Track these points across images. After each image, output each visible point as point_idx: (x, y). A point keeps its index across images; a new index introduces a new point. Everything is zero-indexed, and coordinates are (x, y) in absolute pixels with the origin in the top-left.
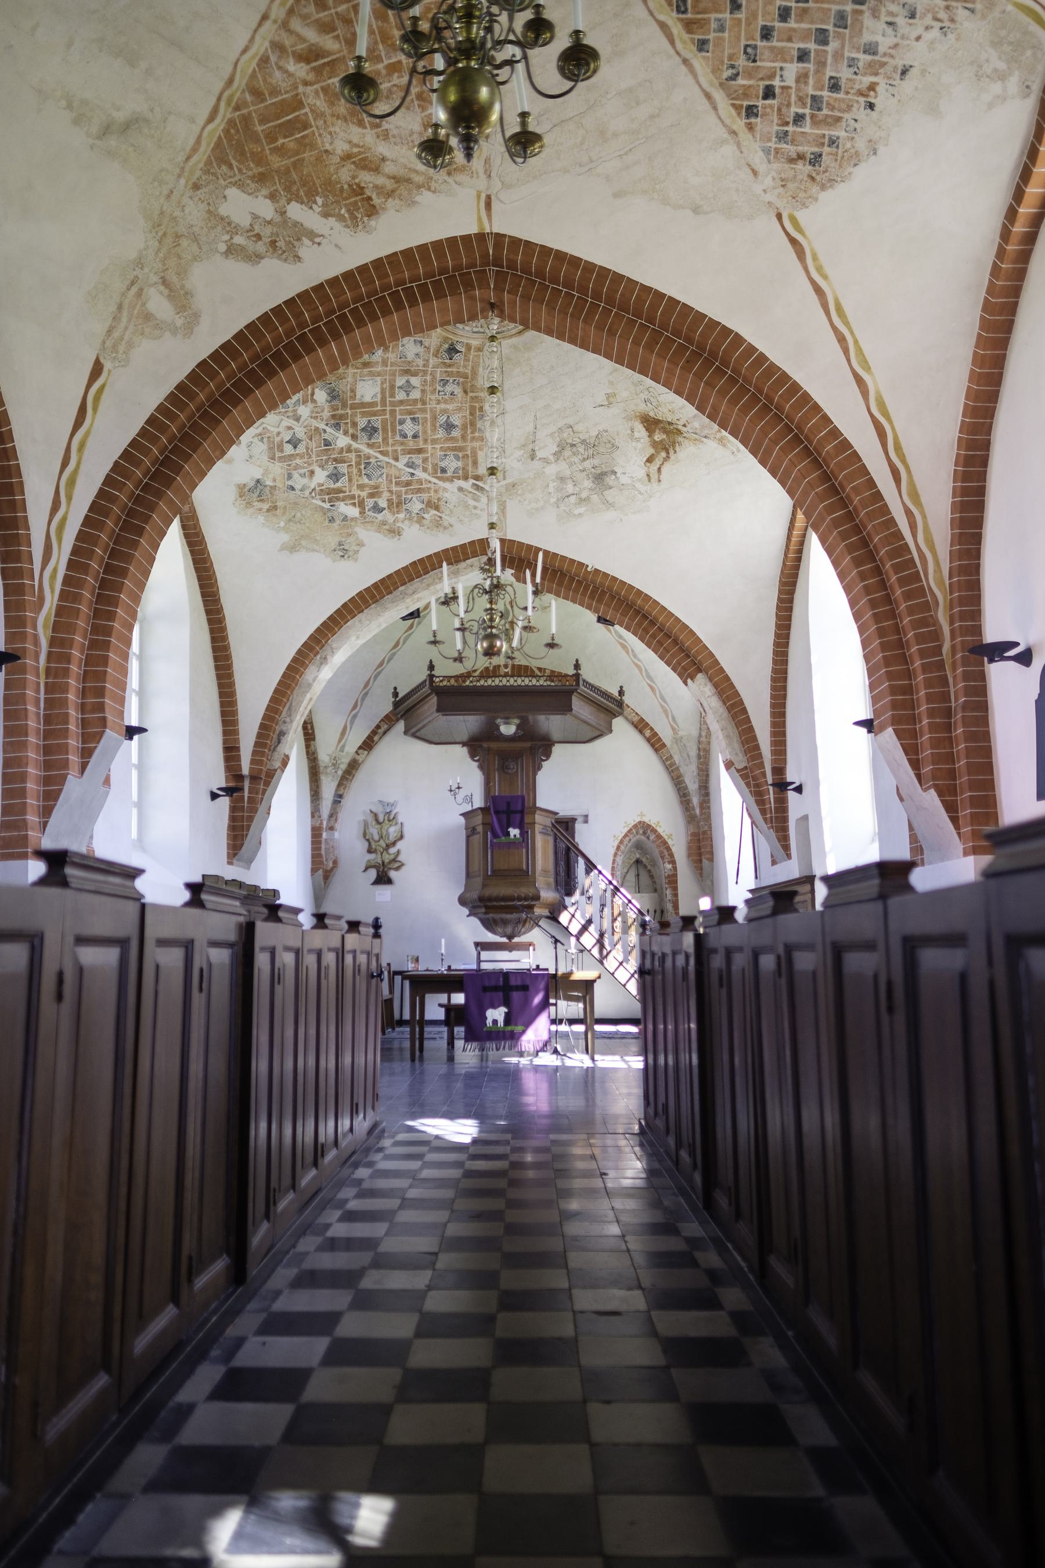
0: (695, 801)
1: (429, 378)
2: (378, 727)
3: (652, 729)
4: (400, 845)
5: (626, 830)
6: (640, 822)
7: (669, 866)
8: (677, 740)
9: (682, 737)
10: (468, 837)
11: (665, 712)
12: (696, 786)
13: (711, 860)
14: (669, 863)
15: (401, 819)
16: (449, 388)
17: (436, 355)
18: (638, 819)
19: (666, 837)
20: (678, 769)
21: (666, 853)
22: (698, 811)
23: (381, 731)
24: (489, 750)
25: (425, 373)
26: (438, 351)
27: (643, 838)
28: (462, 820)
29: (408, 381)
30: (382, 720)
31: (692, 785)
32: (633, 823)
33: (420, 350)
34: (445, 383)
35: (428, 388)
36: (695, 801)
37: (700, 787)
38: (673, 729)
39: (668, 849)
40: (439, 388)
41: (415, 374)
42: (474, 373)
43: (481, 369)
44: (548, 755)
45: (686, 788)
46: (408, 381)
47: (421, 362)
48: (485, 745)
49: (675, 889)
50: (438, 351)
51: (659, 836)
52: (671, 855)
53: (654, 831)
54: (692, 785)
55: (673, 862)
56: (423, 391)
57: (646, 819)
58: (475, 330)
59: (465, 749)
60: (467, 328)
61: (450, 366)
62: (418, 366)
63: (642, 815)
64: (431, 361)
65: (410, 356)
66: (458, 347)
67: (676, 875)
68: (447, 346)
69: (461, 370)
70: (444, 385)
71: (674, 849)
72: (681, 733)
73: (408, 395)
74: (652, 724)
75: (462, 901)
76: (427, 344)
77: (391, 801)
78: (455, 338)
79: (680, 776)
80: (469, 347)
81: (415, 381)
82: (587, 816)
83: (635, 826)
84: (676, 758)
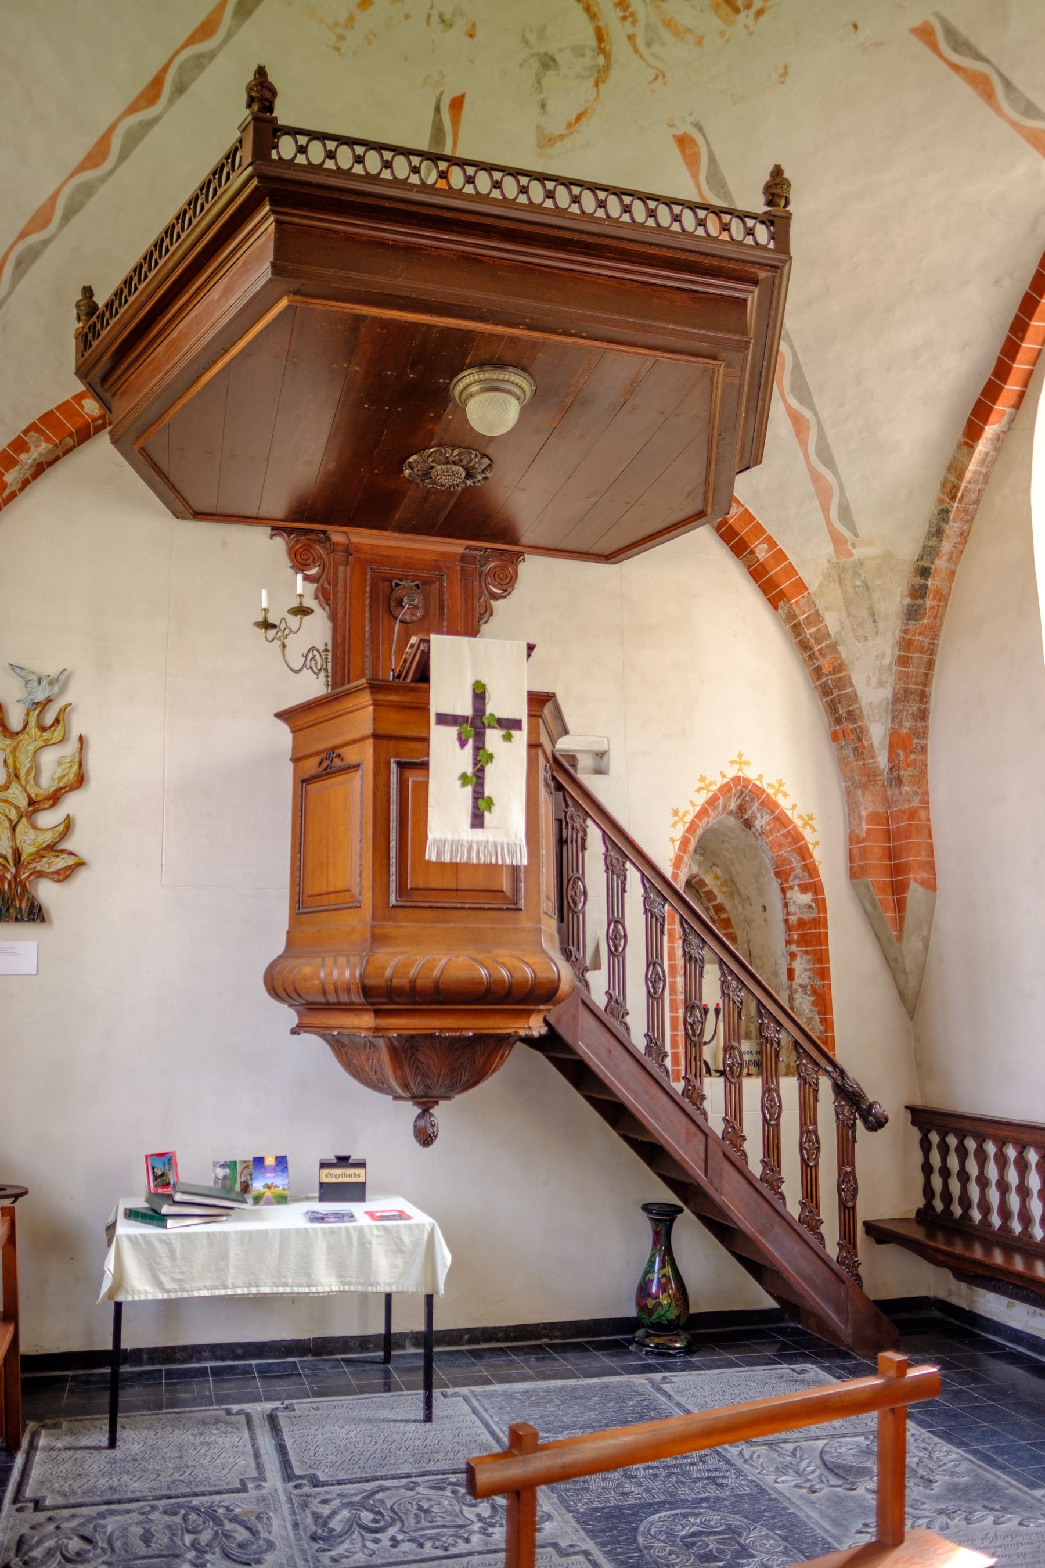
0: (877, 732)
2: (19, 445)
3: (771, 542)
4: (71, 804)
5: (702, 798)
6: (737, 779)
7: (807, 898)
8: (842, 571)
9: (861, 563)
10: (304, 782)
11: (823, 493)
12: (886, 693)
13: (931, 885)
14: (804, 889)
15: (78, 725)
18: (732, 772)
19: (799, 823)
20: (834, 647)
21: (796, 863)
22: (882, 760)
23: (27, 459)
24: (348, 550)
27: (732, 822)
28: (283, 736)
30: (32, 427)
31: (872, 688)
32: (720, 782)
36: (877, 732)
37: (900, 697)
38: (837, 539)
39: (804, 853)
44: (508, 582)
45: (854, 698)
48: (338, 535)
49: (821, 958)
51: (781, 820)
52: (811, 869)
53: (769, 805)
54: (872, 688)
55: (814, 888)
57: (750, 773)
59: (280, 544)
63: (740, 761)
67: (820, 922)
71: (817, 854)
72: (858, 553)
74: (770, 531)
75: (278, 985)
77: (51, 669)
79: (839, 667)
82: (601, 755)
83: (725, 789)
84: (832, 621)
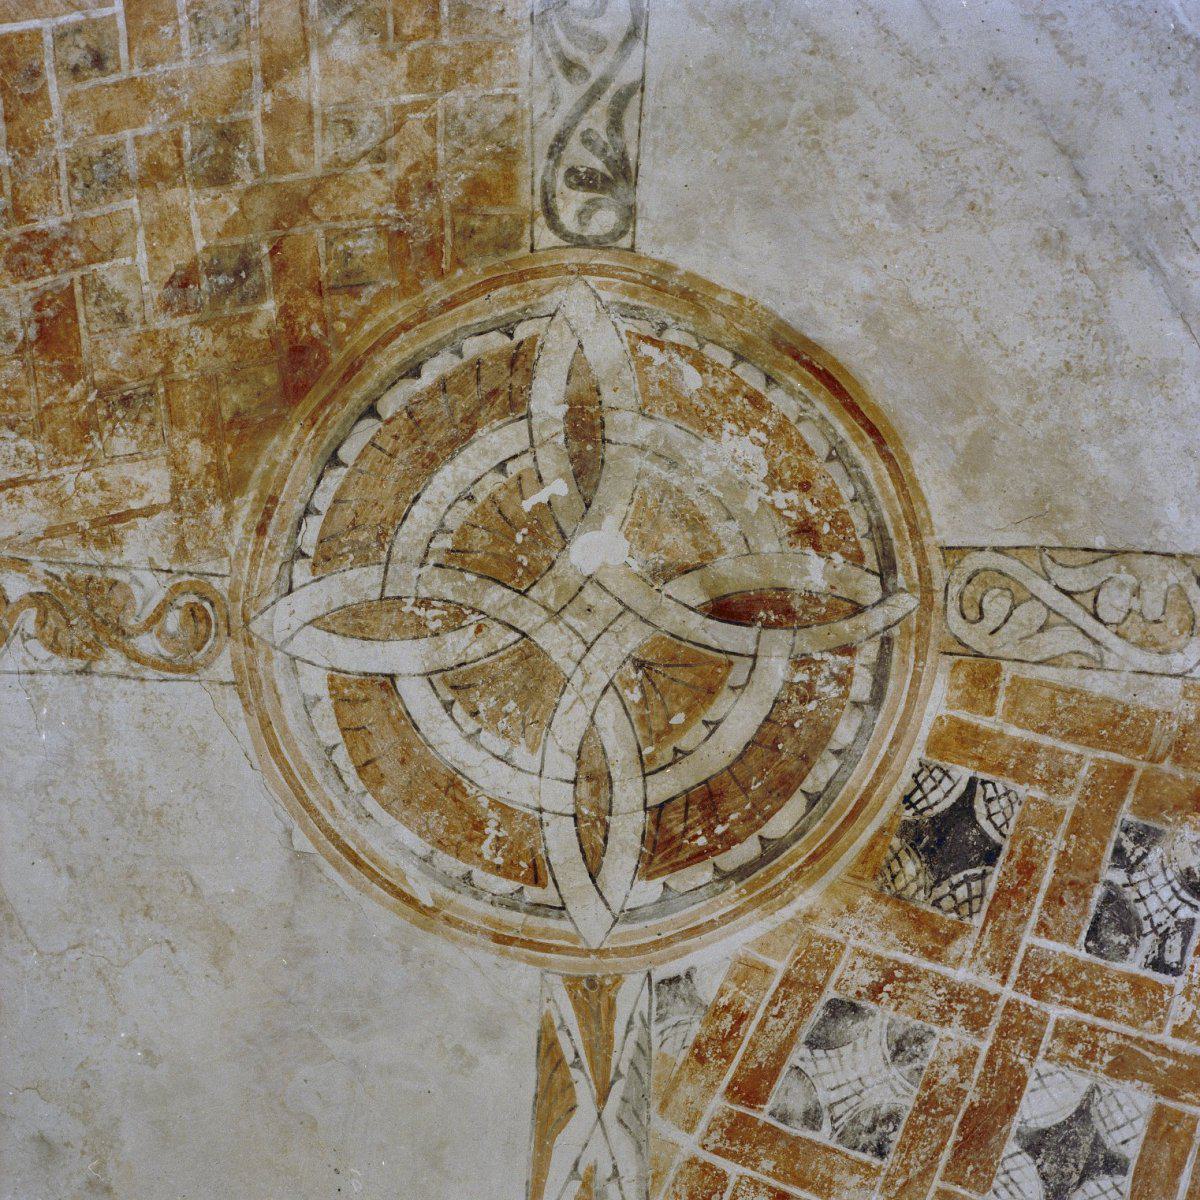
1: (1057, 1012)
16: (1156, 897)
17: (938, 940)
25: (1020, 1027)
26: (920, 921)
29: (1034, 1144)
33: (882, 1019)
34: (1118, 915)
35: (1115, 1030)
40: (1134, 964)
41: (1008, 1086)
42: (1112, 725)
43: (1098, 685)
46: (1034, 1144)
47: (953, 1037)
50: (920, 921)
56: (1124, 1065)
58: (861, 688)
60: (844, 733)
61: (1027, 870)
62: (965, 1060)
64: (961, 975)
65: (890, 1089)
66: (940, 799)
68: (911, 867)
69: (1069, 803)
70: (1129, 924)
73: (1113, 1164)
76: (866, 979)
78: (887, 810)
80: (955, 739)
81: (1046, 1101)
